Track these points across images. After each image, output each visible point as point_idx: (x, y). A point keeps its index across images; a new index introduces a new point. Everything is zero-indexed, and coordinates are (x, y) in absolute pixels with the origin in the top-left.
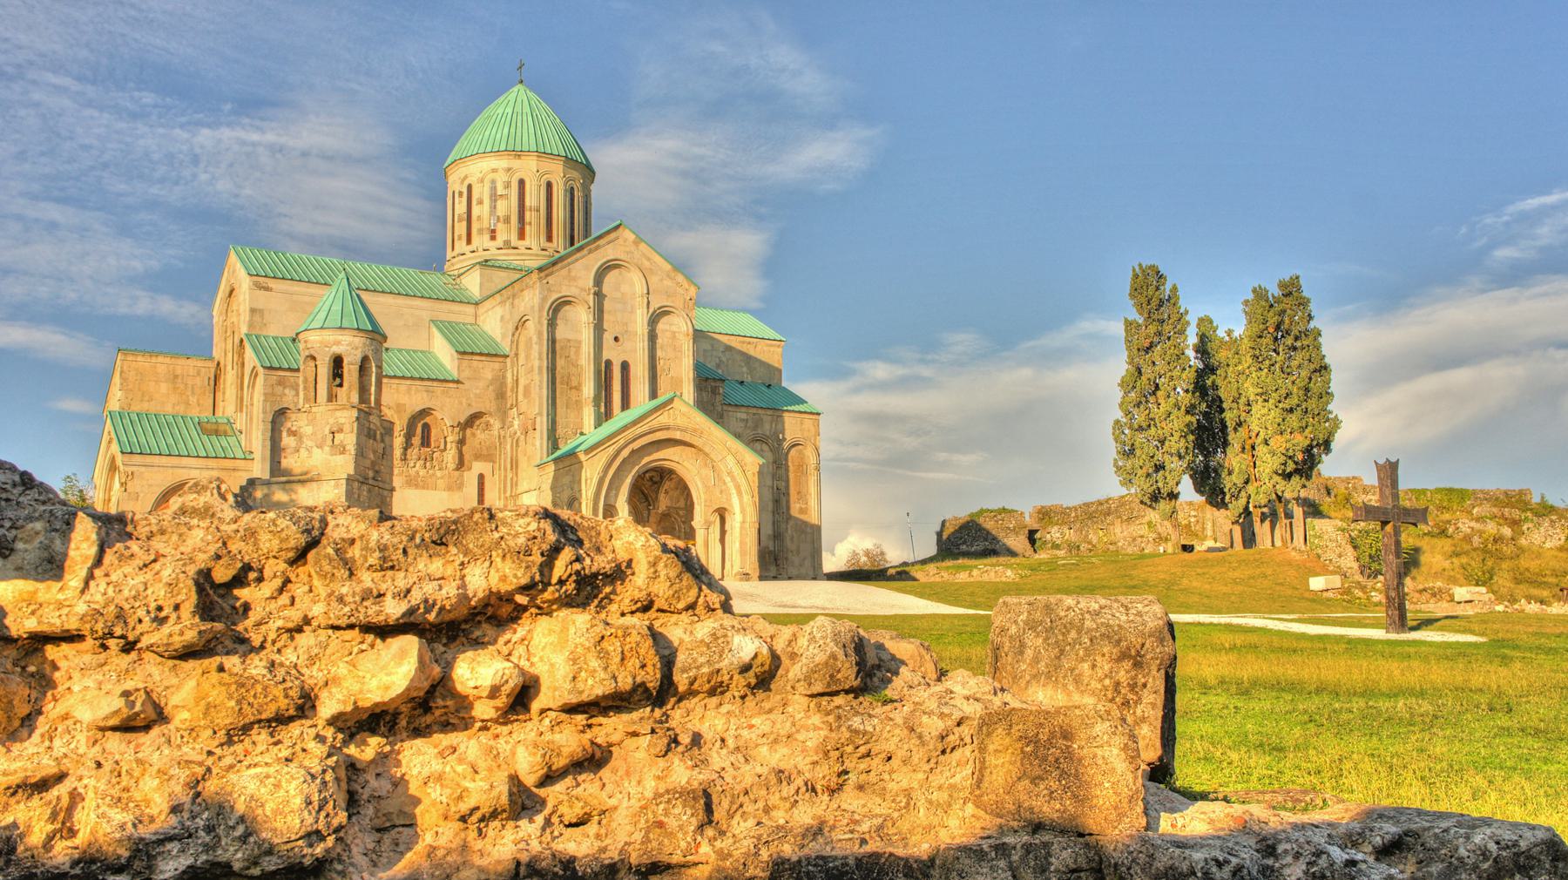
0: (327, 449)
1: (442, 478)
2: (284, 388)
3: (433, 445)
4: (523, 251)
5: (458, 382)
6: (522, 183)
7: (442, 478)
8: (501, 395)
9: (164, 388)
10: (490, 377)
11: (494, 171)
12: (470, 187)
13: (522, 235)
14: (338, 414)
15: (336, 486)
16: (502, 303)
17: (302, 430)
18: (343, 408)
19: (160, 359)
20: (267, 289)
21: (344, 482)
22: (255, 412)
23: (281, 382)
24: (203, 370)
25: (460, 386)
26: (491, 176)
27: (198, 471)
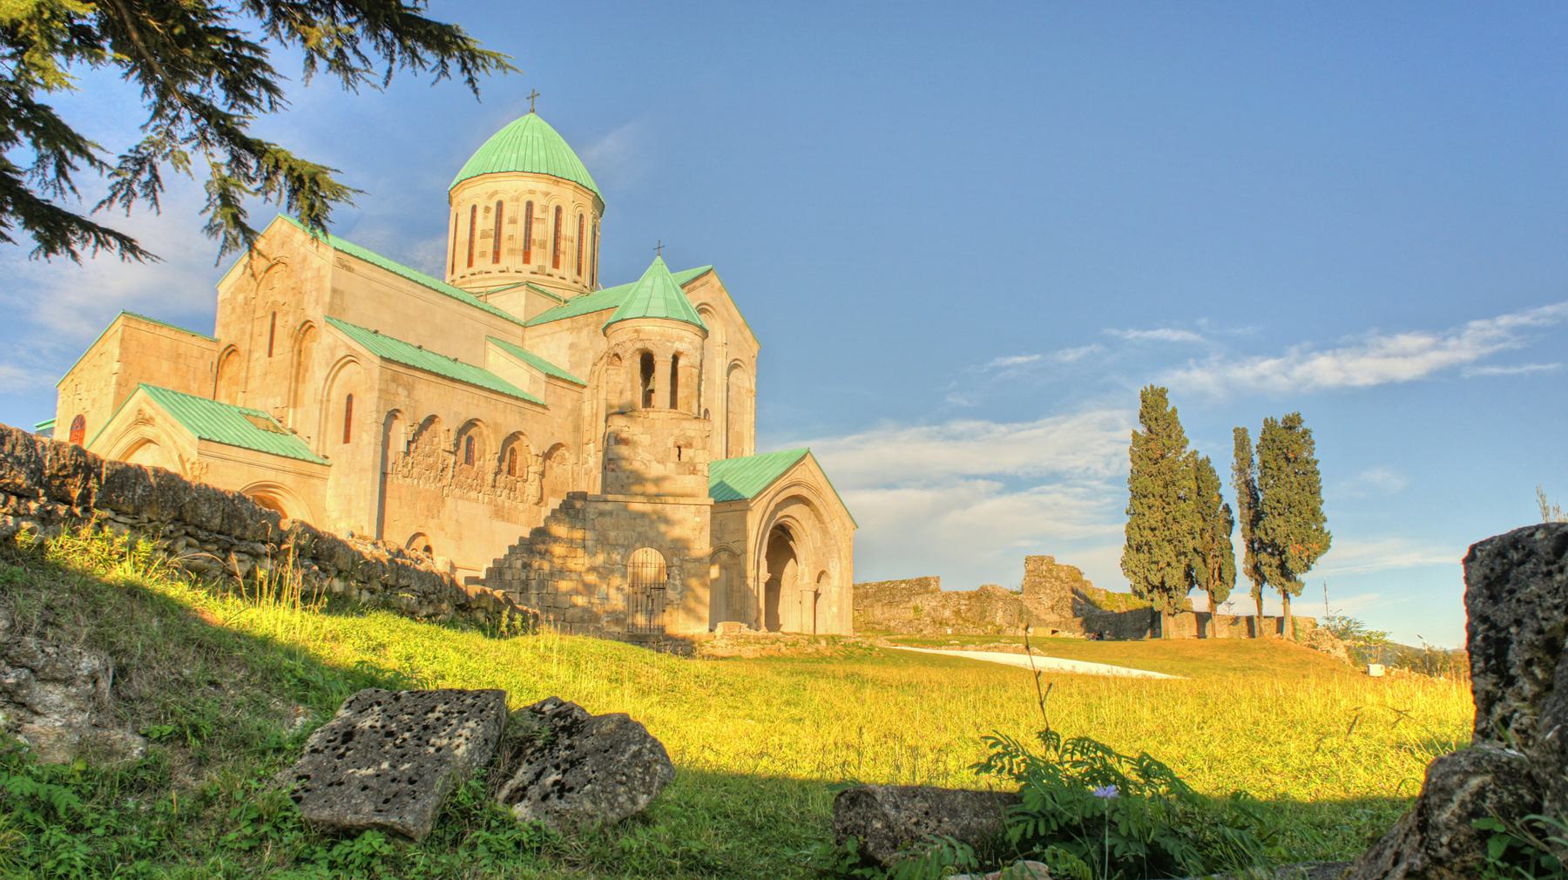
0: (671, 466)
1: (524, 511)
2: (398, 385)
3: (517, 474)
4: (556, 279)
5: (544, 407)
6: (558, 210)
7: (524, 511)
8: (577, 429)
9: (165, 366)
10: (569, 407)
11: (532, 192)
12: (500, 204)
13: (556, 264)
14: (686, 424)
15: (698, 513)
16: (571, 330)
17: (635, 438)
18: (687, 417)
19: (165, 331)
20: (350, 269)
21: (709, 508)
22: (331, 410)
23: (395, 379)
24: (207, 352)
25: (545, 411)
26: (529, 197)
27: (274, 473)
